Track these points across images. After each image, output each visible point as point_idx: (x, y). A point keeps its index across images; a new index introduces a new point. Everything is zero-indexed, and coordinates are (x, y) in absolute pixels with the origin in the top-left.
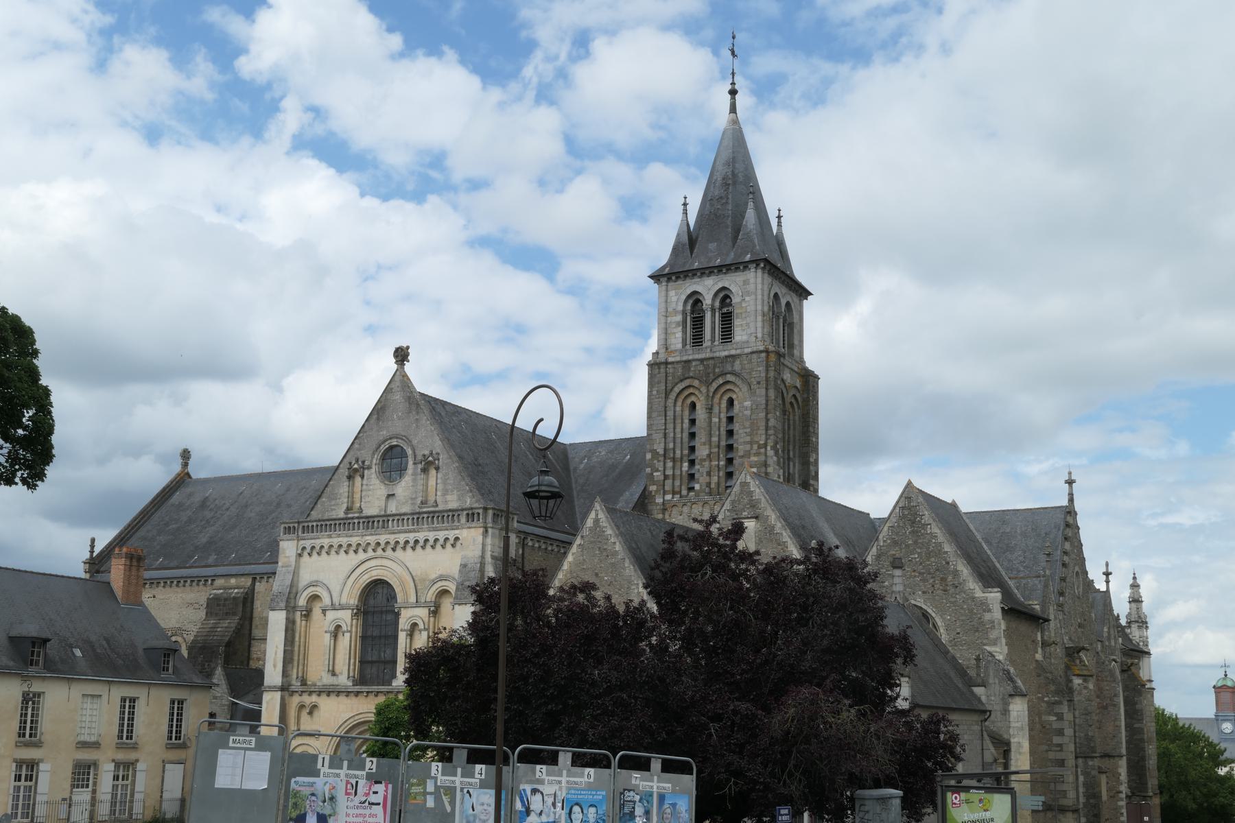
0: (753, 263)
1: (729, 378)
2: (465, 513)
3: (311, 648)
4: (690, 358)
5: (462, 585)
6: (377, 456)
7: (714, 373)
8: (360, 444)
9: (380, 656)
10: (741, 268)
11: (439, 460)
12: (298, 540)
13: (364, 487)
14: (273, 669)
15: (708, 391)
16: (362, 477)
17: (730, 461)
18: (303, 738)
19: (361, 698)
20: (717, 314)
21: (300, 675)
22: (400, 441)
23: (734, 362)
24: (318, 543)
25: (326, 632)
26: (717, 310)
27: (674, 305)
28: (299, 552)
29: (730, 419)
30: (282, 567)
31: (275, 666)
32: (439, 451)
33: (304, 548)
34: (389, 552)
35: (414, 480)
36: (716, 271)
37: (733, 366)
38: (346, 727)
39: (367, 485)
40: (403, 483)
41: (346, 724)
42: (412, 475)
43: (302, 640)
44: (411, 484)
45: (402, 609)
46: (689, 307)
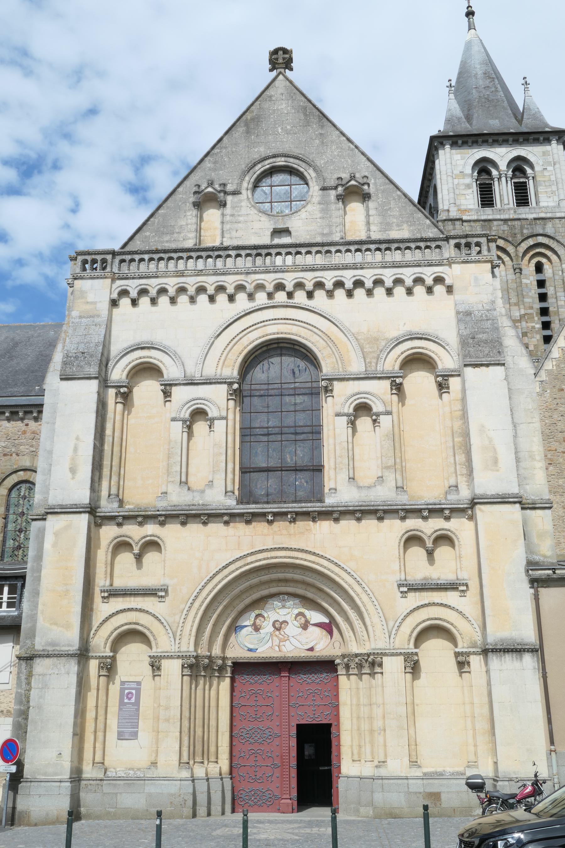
0: (555, 135)
1: (541, 239)
2: (452, 242)
3: (130, 449)
4: (490, 217)
5: (473, 338)
6: (247, 182)
7: (522, 233)
8: (215, 163)
9: (282, 459)
10: (542, 138)
11: (369, 185)
12: (113, 280)
13: (228, 218)
14: (70, 475)
15: (516, 250)
16: (223, 205)
17: (546, 325)
18: (128, 599)
19: (260, 527)
20: (509, 182)
21: (114, 491)
22: (291, 160)
23: (545, 225)
24: (153, 285)
25: (174, 420)
26: (509, 179)
27: (460, 168)
28: (115, 296)
29: (541, 284)
30: (80, 317)
31: (73, 471)
32: (366, 174)
33: (124, 293)
34: (300, 297)
35: (325, 211)
36: (511, 139)
37: (544, 229)
38: (233, 572)
39: (232, 215)
40: (303, 214)
41: (226, 571)
42: (319, 203)
43: (117, 434)
44: (319, 215)
45: (335, 383)
46: (476, 174)
